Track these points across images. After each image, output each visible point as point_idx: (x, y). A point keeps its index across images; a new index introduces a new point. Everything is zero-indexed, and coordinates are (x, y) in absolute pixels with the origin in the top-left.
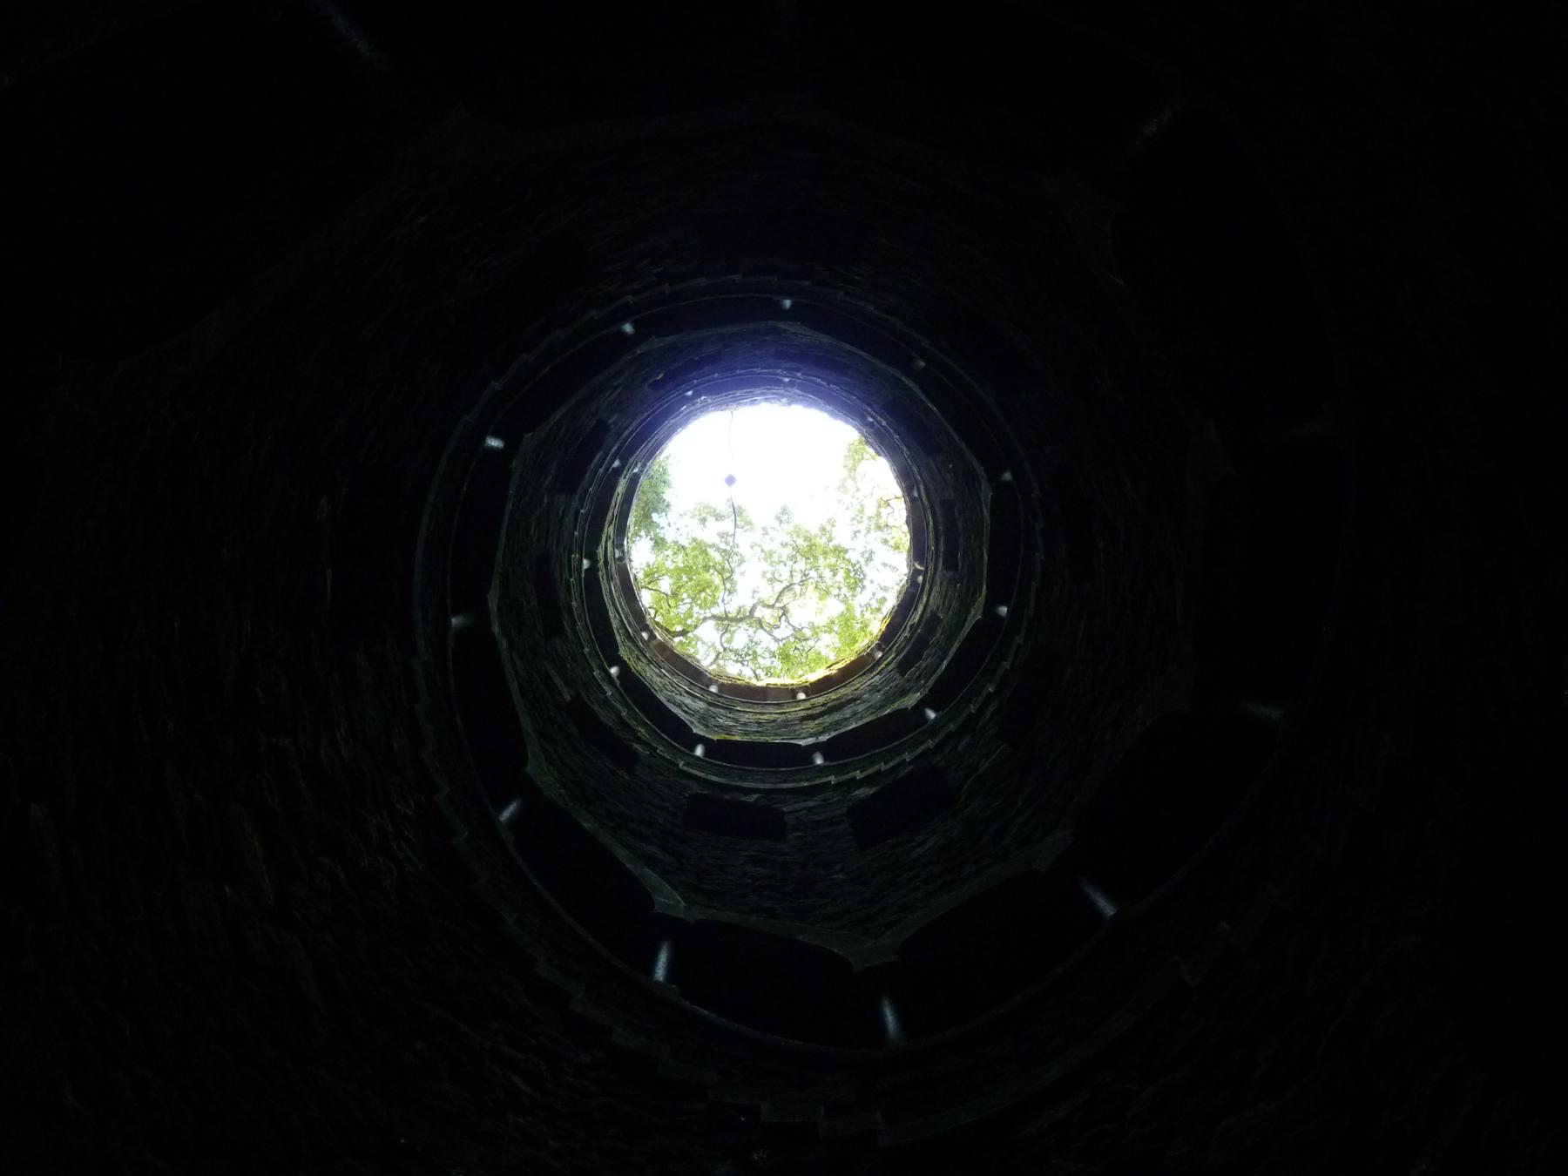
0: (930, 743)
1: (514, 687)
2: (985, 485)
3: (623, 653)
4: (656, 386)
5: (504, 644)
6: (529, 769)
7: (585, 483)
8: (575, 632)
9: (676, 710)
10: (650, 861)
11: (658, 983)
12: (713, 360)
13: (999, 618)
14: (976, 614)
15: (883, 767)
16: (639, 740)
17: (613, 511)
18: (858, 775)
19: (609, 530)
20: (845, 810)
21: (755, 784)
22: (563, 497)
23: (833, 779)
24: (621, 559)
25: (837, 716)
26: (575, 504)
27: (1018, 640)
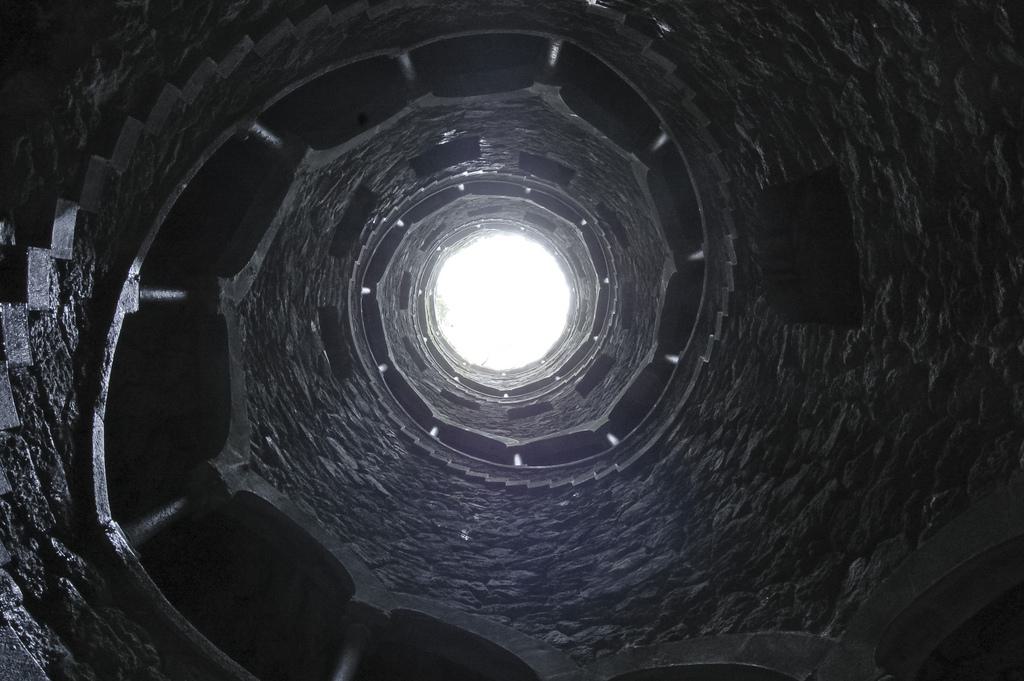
0: (599, 347)
1: (415, 390)
2: (577, 230)
4: (423, 249)
5: (403, 374)
12: (442, 227)
13: (607, 284)
14: (598, 288)
15: (584, 366)
16: (478, 399)
17: (428, 314)
18: (575, 374)
19: (429, 323)
20: (574, 388)
21: (533, 399)
23: (566, 381)
24: (440, 335)
26: (410, 313)
27: (616, 287)
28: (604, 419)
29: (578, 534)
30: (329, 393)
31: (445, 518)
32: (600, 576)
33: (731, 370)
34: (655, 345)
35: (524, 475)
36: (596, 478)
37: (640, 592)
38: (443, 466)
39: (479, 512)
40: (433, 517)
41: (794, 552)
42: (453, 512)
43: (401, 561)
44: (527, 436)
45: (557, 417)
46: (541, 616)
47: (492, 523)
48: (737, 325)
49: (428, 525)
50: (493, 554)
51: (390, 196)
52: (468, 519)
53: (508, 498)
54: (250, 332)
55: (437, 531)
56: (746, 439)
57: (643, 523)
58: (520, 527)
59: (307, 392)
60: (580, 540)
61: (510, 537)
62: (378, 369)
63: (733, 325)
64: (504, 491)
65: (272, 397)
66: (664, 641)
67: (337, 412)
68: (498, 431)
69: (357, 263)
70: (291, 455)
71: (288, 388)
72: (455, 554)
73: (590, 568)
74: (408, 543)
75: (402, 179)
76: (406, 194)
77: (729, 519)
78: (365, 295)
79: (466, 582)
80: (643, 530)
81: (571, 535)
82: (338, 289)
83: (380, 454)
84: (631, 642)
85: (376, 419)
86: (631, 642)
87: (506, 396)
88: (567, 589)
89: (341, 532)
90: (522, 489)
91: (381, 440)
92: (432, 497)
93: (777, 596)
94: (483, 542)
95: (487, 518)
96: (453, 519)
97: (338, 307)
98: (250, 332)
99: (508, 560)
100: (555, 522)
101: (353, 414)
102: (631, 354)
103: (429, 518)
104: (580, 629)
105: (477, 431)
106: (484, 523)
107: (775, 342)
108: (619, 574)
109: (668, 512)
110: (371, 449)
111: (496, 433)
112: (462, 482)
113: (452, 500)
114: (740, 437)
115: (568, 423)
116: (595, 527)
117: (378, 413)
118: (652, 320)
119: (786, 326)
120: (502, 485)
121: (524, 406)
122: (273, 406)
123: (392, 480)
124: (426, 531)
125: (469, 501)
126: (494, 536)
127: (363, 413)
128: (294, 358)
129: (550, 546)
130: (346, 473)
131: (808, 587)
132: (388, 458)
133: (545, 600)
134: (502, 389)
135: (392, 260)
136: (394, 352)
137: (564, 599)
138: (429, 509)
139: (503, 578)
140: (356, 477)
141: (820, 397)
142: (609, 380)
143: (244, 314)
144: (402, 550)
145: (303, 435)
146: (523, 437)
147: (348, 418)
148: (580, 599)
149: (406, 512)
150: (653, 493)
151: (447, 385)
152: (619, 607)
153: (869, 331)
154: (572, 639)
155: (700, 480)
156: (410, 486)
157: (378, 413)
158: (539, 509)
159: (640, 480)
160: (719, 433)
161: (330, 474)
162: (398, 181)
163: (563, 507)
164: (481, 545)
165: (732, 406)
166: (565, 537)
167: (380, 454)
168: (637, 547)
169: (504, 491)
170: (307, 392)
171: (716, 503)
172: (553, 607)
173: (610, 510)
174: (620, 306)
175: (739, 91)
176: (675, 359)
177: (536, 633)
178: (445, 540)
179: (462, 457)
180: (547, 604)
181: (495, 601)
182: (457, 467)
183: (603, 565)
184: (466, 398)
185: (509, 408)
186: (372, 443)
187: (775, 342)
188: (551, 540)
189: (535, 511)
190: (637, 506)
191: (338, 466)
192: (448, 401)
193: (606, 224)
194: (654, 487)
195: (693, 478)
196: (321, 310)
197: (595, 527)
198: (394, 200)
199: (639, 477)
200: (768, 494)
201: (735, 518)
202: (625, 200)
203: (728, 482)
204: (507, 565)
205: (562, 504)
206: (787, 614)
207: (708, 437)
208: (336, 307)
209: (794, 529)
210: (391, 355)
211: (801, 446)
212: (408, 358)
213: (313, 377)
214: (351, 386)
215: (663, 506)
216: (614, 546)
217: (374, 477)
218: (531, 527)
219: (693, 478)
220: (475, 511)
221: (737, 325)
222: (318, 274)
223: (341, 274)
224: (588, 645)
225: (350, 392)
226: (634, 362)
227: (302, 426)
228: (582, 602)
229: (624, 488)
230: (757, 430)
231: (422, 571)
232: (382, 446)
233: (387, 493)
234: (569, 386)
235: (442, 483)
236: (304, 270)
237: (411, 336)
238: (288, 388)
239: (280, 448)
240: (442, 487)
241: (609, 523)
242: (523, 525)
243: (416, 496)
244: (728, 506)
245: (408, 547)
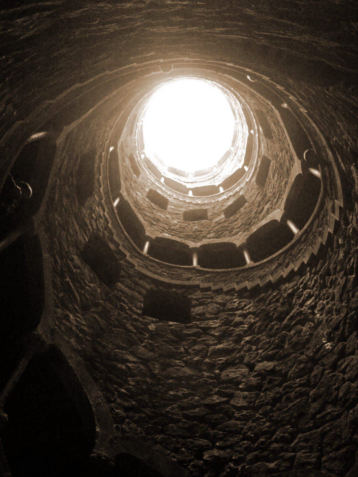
3: (217, 184)
5: (205, 241)
6: (238, 246)
7: (165, 196)
8: (207, 205)
9: (234, 171)
11: (298, 233)
21: (256, 161)
22: (169, 206)
30: (195, 343)
31: (308, 341)
35: (305, 240)
36: (338, 220)
38: (270, 286)
40: (303, 347)
50: (350, 350)
51: (96, 220)
53: (316, 273)
54: (137, 416)
55: (314, 361)
58: (341, 301)
59: (188, 371)
62: (194, 268)
64: (308, 269)
65: (179, 421)
67: (208, 346)
68: (266, 207)
69: (128, 258)
70: (221, 439)
74: (314, 400)
75: (88, 211)
76: (100, 204)
82: (137, 284)
83: (245, 332)
85: (224, 305)
90: (314, 260)
91: (238, 319)
92: (288, 328)
94: (339, 341)
95: (322, 309)
96: (311, 335)
97: (148, 287)
98: (137, 416)
101: (215, 328)
103: (302, 353)
110: (239, 338)
112: (288, 287)
115: (285, 171)
120: (303, 266)
121: (258, 169)
122: (186, 426)
124: (311, 370)
125: (305, 301)
126: (336, 328)
127: (216, 315)
128: (165, 366)
130: (249, 388)
132: (251, 325)
134: (240, 166)
135: (135, 210)
136: (188, 237)
138: (297, 344)
140: (254, 380)
143: (122, 420)
145: (212, 407)
147: (213, 335)
149: (291, 367)
156: (275, 335)
157: (219, 299)
158: (335, 268)
162: (90, 215)
169: (308, 269)
170: (188, 371)
178: (323, 365)
179: (271, 262)
185: (254, 179)
186: (238, 330)
189: (334, 274)
192: (232, 218)
196: (146, 312)
198: (100, 216)
205: (341, 255)
208: (147, 291)
212: (195, 226)
213: (181, 353)
214: (197, 309)
217: (259, 362)
218: (345, 296)
220: (313, 307)
222: (122, 309)
223: (130, 276)
225: (202, 317)
227: (208, 401)
235: (283, 304)
236: (115, 326)
237: (184, 209)
239: (214, 447)
240: (284, 309)
242: (341, 296)
243: (283, 341)
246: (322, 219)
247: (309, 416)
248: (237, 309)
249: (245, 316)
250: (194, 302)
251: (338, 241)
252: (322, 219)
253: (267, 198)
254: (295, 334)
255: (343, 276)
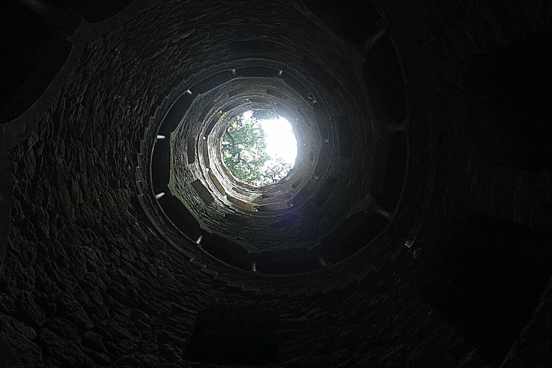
10: (180, 130)
25: (218, 173)
28: (174, 193)
29: (103, 165)
31: (131, 87)
32: (71, 173)
33: (181, 274)
34: (210, 231)
37: (53, 195)
39: (131, 109)
41: (53, 294)
42: (133, 94)
43: (106, 55)
44: (175, 146)
45: (183, 165)
46: (51, 132)
47: (122, 115)
48: (207, 283)
49: (128, 77)
52: (128, 101)
56: (136, 275)
57: (100, 204)
58: (116, 130)
60: (99, 166)
61: (110, 124)
63: (208, 280)
66: (13, 205)
69: (297, 72)
71: (229, 13)
72: (106, 89)
73: (78, 169)
77: (87, 257)
78: (278, 71)
79: (84, 91)
80: (95, 204)
81: (104, 161)
83: (180, 57)
84: (19, 184)
86: (19, 184)
87: (204, 138)
88: (66, 151)
89: (131, 23)
93: (26, 279)
95: (126, 112)
96: (130, 92)
99: (94, 120)
100: (115, 152)
102: (209, 216)
103: (132, 78)
104: (36, 154)
105: (184, 117)
106: (123, 110)
107: (189, 304)
108: (69, 185)
109: (104, 222)
111: (181, 128)
113: (142, 94)
114: (139, 272)
116: (105, 175)
117: (206, 62)
118: (225, 232)
119: (197, 312)
123: (162, 61)
129: (99, 146)
131: (26, 300)
132: (176, 62)
133: (62, 136)
137: (59, 148)
139: (83, 114)
141: (148, 325)
142: (197, 199)
144: (113, 57)
146: (176, 143)
147: (207, 44)
148: (57, 158)
150: (118, 214)
151: (218, 106)
152: (46, 181)
153: (178, 363)
154: (30, 148)
155: (118, 243)
157: (206, 62)
158: (126, 144)
159: (129, 207)
160: (145, 259)
161: (170, 25)
163: (123, 158)
164: (108, 105)
165: (158, 270)
166: (103, 156)
167: (180, 57)
168: (84, 197)
170: (225, 23)
171: (101, 251)
172: (56, 141)
173: (113, 185)
174: (240, 215)
175: (336, 315)
176: (198, 242)
177: (39, 127)
180: (58, 138)
181: (68, 105)
182: (163, 101)
183: (78, 176)
184: (207, 115)
186: (187, 55)
187: (189, 304)
188: (103, 147)
189: (125, 142)
190: (113, 204)
191: (175, 31)
193: (287, 217)
194: (122, 215)
195: (121, 240)
197: (105, 175)
198: (328, 101)
199: (131, 206)
200: (96, 284)
201: (87, 261)
202: (297, 232)
203: (112, 260)
204: (92, 119)
205: (125, 158)
206: (11, 284)
207: (145, 253)
209: (69, 296)
210: (241, 78)
211: (121, 309)
215: (108, 218)
216: (89, 184)
219: (121, 240)
220: (133, 106)
221: (207, 283)
224: (23, 157)
226: (205, 217)
227: (204, 15)
228: (55, 158)
229: (126, 196)
230: (139, 283)
231: (97, 66)
232: (184, 60)
233: (154, 56)
234: (201, 176)
238: (229, 13)
241: (106, 185)
242: (117, 133)
244: (97, 257)
245: (114, 61)
246: (144, 168)
247: (119, 52)
248: (190, 65)
249: (183, 64)
250: (228, 53)
251: (131, 166)
252: (144, 168)
253: (183, 137)
254: (142, 82)
255: (120, 147)
